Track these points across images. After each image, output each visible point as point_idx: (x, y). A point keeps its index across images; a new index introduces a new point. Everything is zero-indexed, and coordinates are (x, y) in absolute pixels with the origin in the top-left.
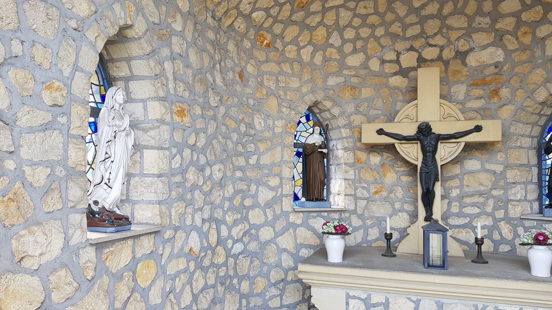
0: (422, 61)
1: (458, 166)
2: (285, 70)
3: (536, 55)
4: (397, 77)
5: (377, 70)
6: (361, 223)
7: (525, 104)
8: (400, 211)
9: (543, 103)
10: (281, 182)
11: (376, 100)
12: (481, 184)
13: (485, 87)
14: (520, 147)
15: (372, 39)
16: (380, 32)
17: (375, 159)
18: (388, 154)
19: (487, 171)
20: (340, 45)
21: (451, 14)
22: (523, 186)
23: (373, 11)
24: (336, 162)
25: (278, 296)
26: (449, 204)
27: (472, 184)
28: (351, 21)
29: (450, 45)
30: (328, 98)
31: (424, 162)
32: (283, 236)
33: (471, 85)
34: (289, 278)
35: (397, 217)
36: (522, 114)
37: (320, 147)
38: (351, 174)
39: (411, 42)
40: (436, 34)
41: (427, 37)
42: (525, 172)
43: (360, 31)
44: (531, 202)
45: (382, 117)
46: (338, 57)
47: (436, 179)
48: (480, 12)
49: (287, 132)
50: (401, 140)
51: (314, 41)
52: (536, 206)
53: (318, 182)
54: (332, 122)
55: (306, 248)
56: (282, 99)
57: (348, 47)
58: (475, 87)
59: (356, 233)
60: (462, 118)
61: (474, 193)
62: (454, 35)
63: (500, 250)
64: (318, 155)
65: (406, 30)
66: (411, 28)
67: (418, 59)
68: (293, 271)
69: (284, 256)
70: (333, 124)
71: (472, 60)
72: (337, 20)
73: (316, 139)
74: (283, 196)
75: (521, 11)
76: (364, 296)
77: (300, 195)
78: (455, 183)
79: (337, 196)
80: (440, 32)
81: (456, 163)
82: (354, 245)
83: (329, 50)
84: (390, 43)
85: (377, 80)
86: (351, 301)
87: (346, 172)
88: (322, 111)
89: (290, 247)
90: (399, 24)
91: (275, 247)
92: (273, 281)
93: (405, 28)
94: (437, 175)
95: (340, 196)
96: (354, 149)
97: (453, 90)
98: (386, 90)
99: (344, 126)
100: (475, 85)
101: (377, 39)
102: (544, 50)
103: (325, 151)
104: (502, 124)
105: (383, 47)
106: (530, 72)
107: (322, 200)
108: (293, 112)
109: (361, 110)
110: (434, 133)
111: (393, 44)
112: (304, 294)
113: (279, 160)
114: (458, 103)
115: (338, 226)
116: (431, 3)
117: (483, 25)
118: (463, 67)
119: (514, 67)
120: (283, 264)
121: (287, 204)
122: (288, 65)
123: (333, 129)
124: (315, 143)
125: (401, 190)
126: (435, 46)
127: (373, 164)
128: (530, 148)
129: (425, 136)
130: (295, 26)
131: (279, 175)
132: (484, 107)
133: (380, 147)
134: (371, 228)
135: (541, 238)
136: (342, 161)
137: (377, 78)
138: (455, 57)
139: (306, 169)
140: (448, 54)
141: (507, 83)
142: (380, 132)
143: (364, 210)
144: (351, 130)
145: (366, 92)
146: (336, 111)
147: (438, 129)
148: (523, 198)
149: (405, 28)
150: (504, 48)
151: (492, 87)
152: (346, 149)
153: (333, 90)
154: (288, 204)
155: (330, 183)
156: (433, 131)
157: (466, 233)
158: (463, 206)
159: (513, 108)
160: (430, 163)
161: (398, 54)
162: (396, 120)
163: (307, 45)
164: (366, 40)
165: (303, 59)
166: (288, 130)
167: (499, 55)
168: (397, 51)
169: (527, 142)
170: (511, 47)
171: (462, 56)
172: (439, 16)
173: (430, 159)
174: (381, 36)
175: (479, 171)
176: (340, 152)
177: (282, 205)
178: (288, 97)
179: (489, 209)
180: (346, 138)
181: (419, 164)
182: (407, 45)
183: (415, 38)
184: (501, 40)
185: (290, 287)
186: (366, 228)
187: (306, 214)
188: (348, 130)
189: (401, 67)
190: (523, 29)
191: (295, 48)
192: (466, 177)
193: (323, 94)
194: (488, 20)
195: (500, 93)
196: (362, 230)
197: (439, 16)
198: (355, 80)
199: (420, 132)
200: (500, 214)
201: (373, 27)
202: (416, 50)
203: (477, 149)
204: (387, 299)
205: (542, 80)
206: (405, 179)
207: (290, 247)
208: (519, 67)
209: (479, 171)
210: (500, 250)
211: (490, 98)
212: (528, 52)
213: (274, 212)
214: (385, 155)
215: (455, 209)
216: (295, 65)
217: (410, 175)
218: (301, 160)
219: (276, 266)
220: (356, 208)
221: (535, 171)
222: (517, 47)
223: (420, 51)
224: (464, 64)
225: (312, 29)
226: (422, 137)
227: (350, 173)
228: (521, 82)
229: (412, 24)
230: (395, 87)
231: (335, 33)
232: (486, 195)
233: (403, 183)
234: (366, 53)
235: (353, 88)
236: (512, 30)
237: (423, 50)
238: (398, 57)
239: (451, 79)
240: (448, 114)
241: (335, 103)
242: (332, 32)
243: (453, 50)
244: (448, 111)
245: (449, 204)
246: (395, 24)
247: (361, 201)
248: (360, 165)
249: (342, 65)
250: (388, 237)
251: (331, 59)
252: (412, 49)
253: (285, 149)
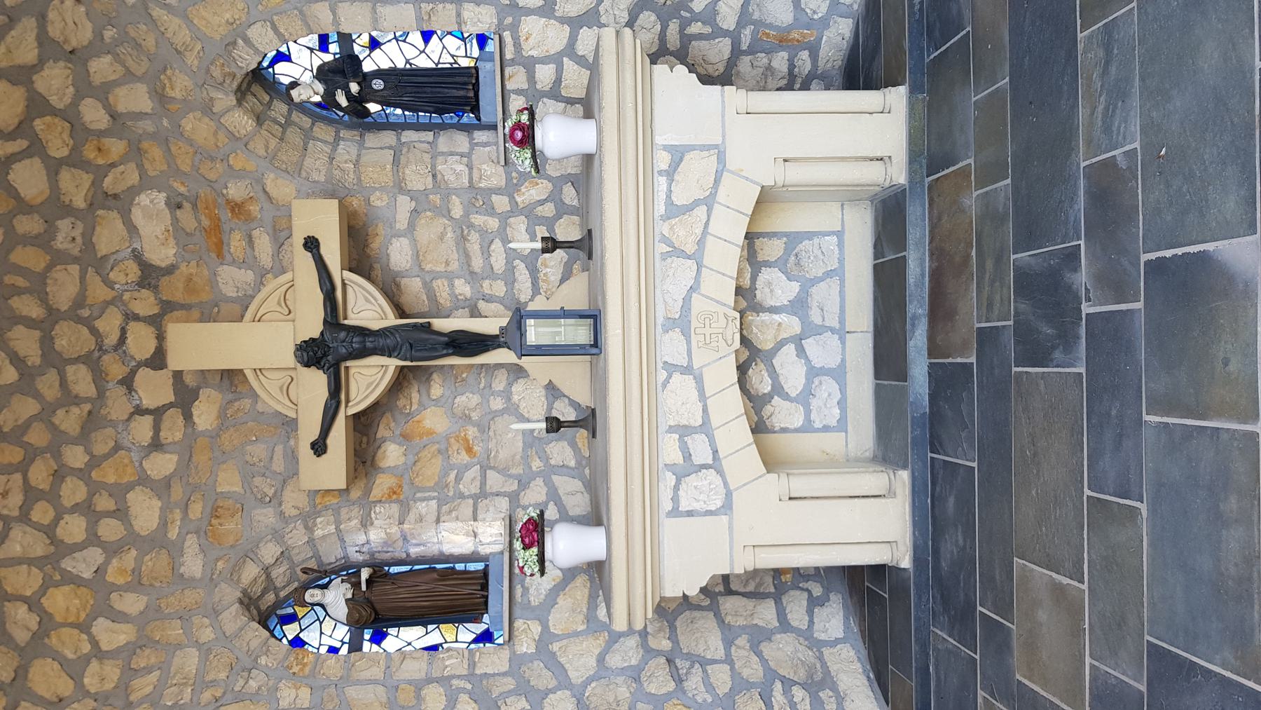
0: (158, 360)
1: (404, 282)
2: (149, 689)
3: (151, 129)
4: (195, 412)
5: (175, 458)
6: (539, 481)
7: (262, 152)
8: (509, 399)
9: (259, 120)
10: (437, 681)
11: (248, 458)
12: (442, 237)
13: (226, 227)
14: (357, 164)
15: (93, 474)
16: (76, 457)
17: (392, 454)
18: (381, 427)
19: (412, 226)
20: (100, 551)
21: (44, 299)
22: (440, 159)
23: (18, 477)
24: (400, 543)
25: (705, 671)
26: (488, 299)
27: (443, 255)
28: (38, 527)
29: (121, 300)
30: (233, 574)
31: (389, 352)
32: (567, 666)
33: (220, 255)
34: (666, 645)
35: (523, 405)
36: (284, 158)
37: (356, 585)
38: (426, 508)
39: (110, 385)
40: (94, 331)
41: (100, 349)
42: (410, 155)
43: (67, 502)
44: (473, 145)
45: (292, 442)
46: (134, 553)
47: (427, 328)
48: (43, 241)
49: (313, 674)
50: (339, 403)
51: (83, 616)
52: (481, 136)
53: (441, 587)
54: (297, 559)
55: (597, 606)
56: (224, 693)
57: (110, 530)
58: (225, 248)
59: (561, 492)
60: (287, 277)
61: (461, 251)
62: (98, 292)
63: (575, 203)
64: (377, 588)
65: (76, 396)
66: (72, 386)
67: (154, 369)
68: (650, 637)
69: (614, 661)
70: (303, 556)
71: (161, 253)
72: (30, 562)
73: (337, 596)
74: (473, 674)
75: (45, 158)
76: (670, 479)
77: (479, 628)
78: (441, 288)
79: (481, 537)
80: (88, 323)
81: (398, 286)
82: (587, 496)
83: (110, 578)
84: (109, 431)
85: (201, 458)
86: (684, 506)
87: (421, 519)
88: (270, 585)
89: (593, 646)
90: (60, 413)
91: (593, 685)
92: (672, 686)
93: (69, 398)
94: (415, 326)
95: (480, 531)
96: (367, 504)
97: (230, 292)
98: (225, 437)
99: (309, 529)
100: (220, 249)
101: (95, 462)
102: (141, 116)
103: (365, 574)
104: (308, 196)
105: (117, 448)
106: (190, 142)
107: (485, 573)
108: (263, 660)
109: (271, 492)
110: (322, 333)
111: (113, 424)
112: (699, 608)
113: (380, 689)
114: (262, 283)
115: (523, 541)
116: (11, 344)
117: (77, 233)
118: (177, 272)
119: (178, 173)
120: (634, 662)
121: (493, 663)
122: (136, 683)
123: (316, 556)
124: (347, 600)
125: (464, 398)
126: (123, 331)
127: (403, 459)
128: (361, 144)
129: (329, 351)
130: (32, 670)
131: (418, 686)
132: (271, 232)
133: (364, 446)
134: (548, 459)
135: (519, 135)
136: (394, 530)
137: (194, 459)
138: (155, 289)
139: (412, 617)
141: (216, 186)
142: (319, 447)
143: (510, 476)
144: (319, 514)
145: (229, 481)
146: (269, 552)
147: (312, 325)
148: (465, 159)
149: (69, 398)
150: (134, 191)
151: (226, 215)
152: (366, 524)
153: (217, 560)
154: (493, 660)
155: (452, 555)
156: (316, 335)
157: (546, 267)
158: (491, 274)
159: (272, 176)
160: (389, 342)
161: (140, 411)
162: (292, 415)
163: (89, 634)
164: (94, 488)
165: (128, 643)
166: (307, 670)
168: (132, 414)
169: (347, 149)
170: (133, 178)
171: (150, 275)
172: (46, 326)
173: (381, 342)
174: (88, 451)
175: (414, 242)
176: (373, 535)
177: (494, 675)
178: (223, 675)
179: (493, 223)
180: (338, 523)
181: (393, 363)
182: (116, 394)
183: (99, 377)
184: (115, 196)
185: (687, 642)
186: (550, 471)
187: (517, 611)
188: (319, 520)
189: (171, 405)
190: (90, 153)
191: (94, 665)
192: (428, 267)
193: (223, 585)
194: (64, 225)
195: (239, 200)
196: (555, 478)
197: (46, 326)
198: (196, 510)
199: (319, 363)
200: (501, 203)
201: (59, 475)
202: (133, 372)
203: (366, 246)
204: (671, 429)
205: (207, 120)
206: (437, 390)
207: (593, 646)
208: (179, 162)
209: (414, 242)
210: (575, 203)
211: (249, 218)
212: (145, 145)
213: (509, 693)
214: (382, 432)
215: (499, 289)
216: (140, 662)
217: (429, 380)
218: (391, 631)
219: (637, 679)
220: (504, 494)
221: (409, 136)
222: (132, 165)
223: (134, 364)
224: (170, 270)
225: (47, 623)
226: (330, 358)
227: (424, 511)
228: (213, 159)
229: (63, 383)
230: (219, 417)
231: (67, 564)
232: (463, 230)
233: (448, 393)
234: (130, 487)
235: (215, 513)
236: (91, 176)
237: (133, 358)
238: (147, 412)
239: (205, 297)
240: (279, 303)
241: (250, 554)
242: (64, 572)
243: (136, 294)
244: (272, 304)
245: (488, 299)
246: (57, 422)
247: (489, 482)
248: (406, 487)
249: (157, 541)
250: (554, 425)
251: (136, 572)
252: (128, 383)
253: (355, 675)
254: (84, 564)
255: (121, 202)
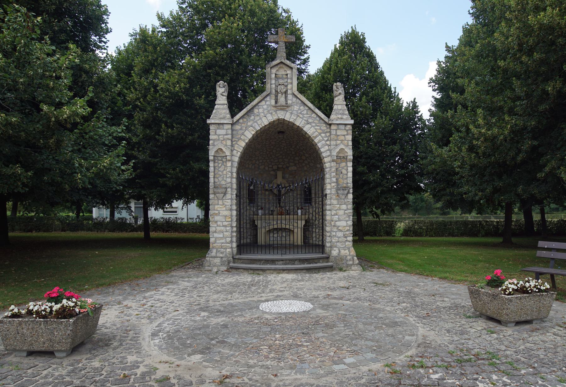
57: (260, 164)
71: (290, 169)
140: (284, 167)
167: (295, 168)
171: (288, 167)
254: (257, 162)
255: (295, 165)
